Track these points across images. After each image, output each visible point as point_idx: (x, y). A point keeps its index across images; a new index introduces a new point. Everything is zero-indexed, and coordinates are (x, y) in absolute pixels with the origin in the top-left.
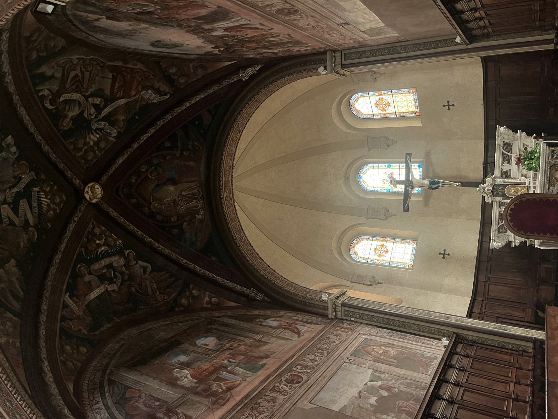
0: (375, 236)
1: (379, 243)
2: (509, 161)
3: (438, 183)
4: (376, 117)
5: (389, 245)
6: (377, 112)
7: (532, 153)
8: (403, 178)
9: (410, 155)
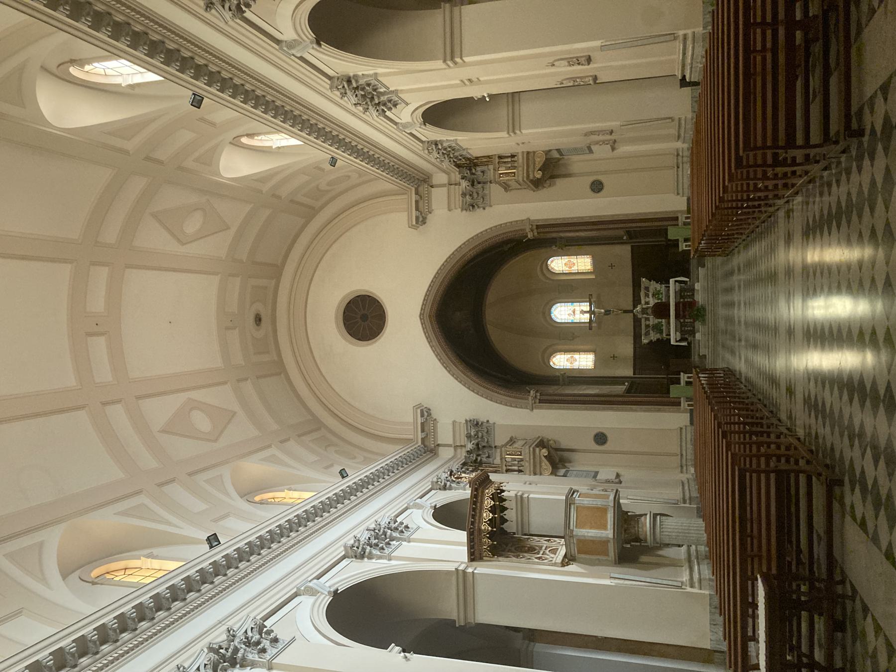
0: (566, 351)
1: (569, 356)
2: (648, 297)
3: (610, 311)
4: (564, 272)
5: (577, 356)
6: (566, 269)
7: (659, 291)
8: (588, 309)
9: (591, 295)
